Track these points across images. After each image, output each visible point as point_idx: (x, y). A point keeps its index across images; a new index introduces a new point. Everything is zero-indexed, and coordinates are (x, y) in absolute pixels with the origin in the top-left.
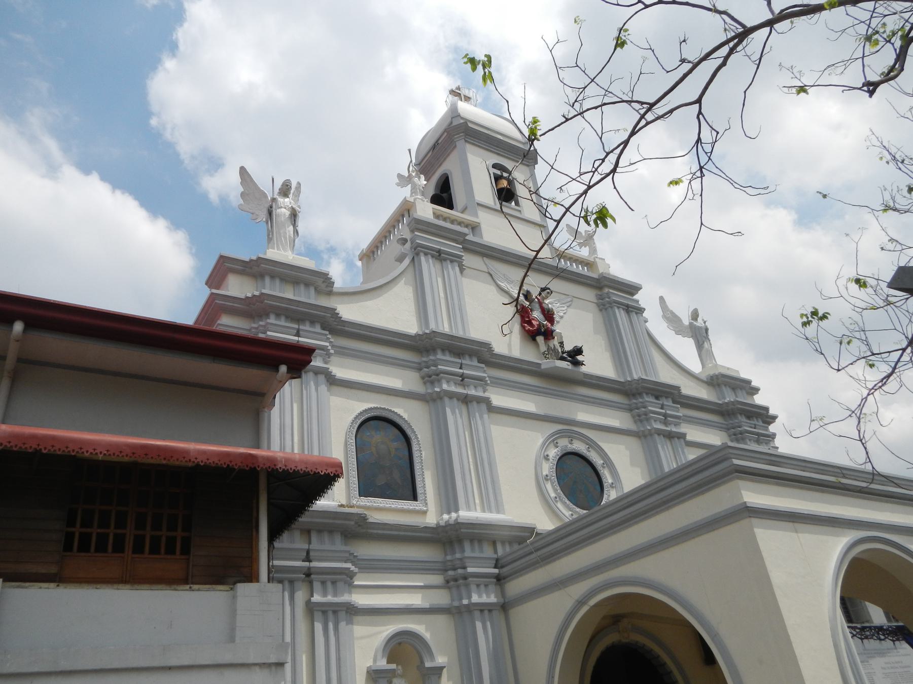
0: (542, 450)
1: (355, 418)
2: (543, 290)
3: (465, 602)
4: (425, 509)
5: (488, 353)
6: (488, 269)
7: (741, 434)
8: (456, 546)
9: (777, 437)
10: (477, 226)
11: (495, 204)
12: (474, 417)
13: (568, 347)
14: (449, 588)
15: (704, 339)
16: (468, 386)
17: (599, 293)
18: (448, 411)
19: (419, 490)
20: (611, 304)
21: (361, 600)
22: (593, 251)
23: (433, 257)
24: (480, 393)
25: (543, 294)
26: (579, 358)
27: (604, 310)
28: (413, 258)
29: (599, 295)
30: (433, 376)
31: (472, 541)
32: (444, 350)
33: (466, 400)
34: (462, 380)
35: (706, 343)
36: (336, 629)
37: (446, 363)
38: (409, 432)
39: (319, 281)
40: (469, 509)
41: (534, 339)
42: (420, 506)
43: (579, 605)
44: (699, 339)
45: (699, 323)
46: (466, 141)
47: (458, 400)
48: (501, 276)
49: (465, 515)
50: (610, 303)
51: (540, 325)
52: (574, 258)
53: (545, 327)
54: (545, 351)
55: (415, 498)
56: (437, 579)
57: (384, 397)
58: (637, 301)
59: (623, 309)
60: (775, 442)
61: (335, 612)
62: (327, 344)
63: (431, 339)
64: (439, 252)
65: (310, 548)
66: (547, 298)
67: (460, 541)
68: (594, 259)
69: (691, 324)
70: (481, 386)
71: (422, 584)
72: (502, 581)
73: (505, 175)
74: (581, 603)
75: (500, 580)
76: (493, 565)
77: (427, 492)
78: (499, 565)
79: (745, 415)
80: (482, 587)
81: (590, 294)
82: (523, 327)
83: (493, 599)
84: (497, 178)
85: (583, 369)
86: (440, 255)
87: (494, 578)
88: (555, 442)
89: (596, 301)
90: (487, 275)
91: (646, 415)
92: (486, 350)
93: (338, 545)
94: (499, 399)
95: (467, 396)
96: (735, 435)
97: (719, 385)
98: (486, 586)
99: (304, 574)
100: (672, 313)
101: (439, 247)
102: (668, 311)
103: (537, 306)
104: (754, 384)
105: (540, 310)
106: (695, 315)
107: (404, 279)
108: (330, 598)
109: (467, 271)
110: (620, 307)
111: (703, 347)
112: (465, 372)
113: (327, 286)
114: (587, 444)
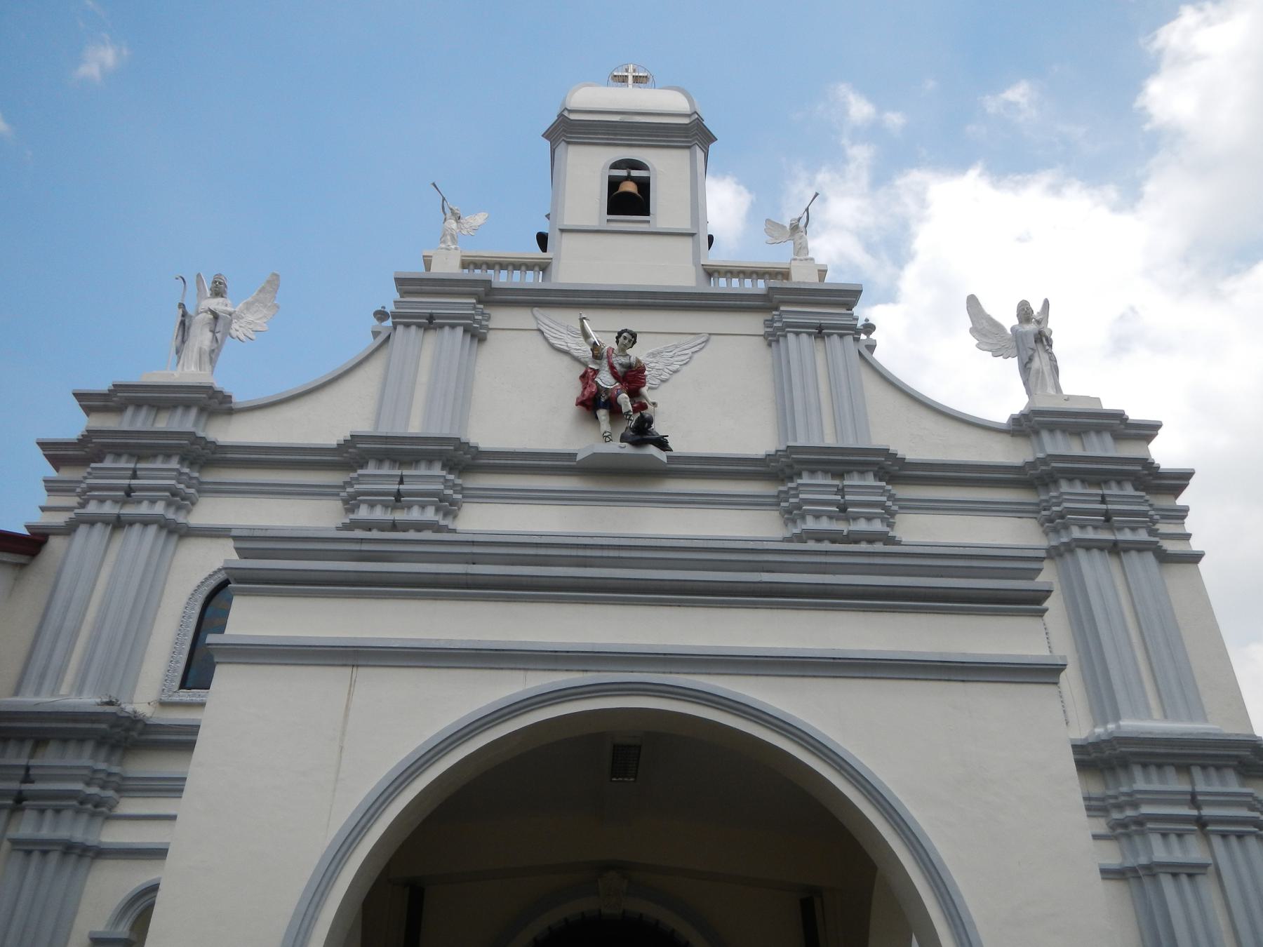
2: (620, 334)
7: (1062, 517)
9: (1189, 513)
23: (419, 326)
25: (621, 339)
27: (774, 344)
28: (389, 336)
29: (767, 320)
46: (569, 143)
48: (562, 330)
53: (610, 395)
54: (605, 432)
59: (809, 334)
60: (1185, 525)
61: (45, 853)
64: (431, 318)
70: (432, 503)
73: (635, 173)
79: (1083, 481)
81: (754, 323)
84: (614, 184)
85: (679, 446)
90: (537, 333)
91: (800, 508)
93: (83, 758)
96: (1051, 521)
97: (1037, 433)
101: (429, 311)
103: (605, 362)
104: (1134, 414)
105: (607, 369)
108: (46, 833)
109: (491, 336)
110: (801, 332)
111: (1030, 368)
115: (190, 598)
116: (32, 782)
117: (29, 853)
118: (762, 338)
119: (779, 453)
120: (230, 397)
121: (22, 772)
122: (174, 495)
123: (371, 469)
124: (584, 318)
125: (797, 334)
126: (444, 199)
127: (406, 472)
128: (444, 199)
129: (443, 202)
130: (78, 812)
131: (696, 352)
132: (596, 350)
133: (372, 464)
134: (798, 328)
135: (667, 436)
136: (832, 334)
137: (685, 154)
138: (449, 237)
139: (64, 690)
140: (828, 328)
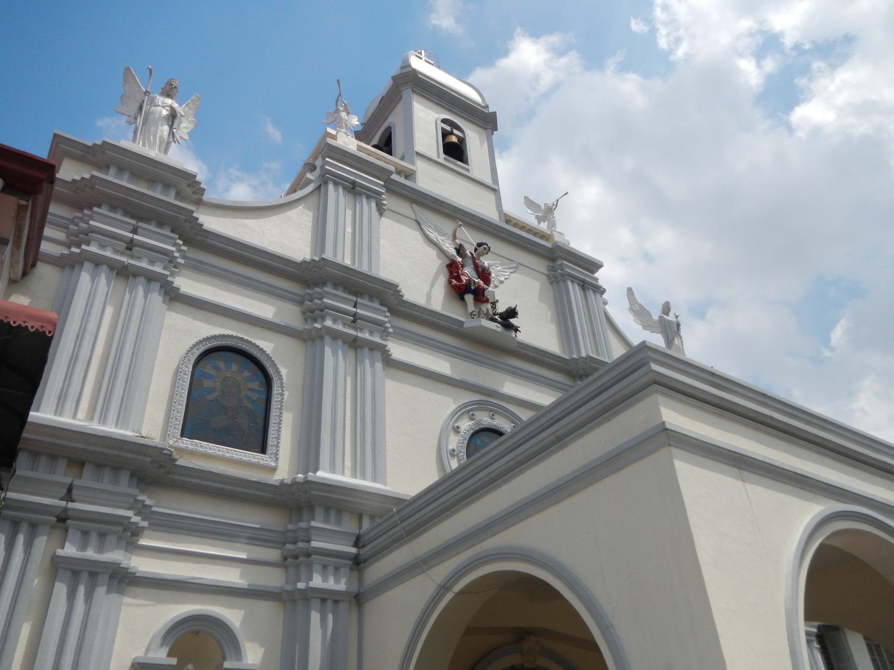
0: (451, 419)
1: (200, 342)
2: (480, 245)
3: (301, 585)
4: (273, 464)
5: (394, 297)
6: (416, 216)
8: (306, 514)
10: (412, 174)
11: (439, 156)
12: (363, 362)
13: (501, 308)
14: (286, 567)
15: (674, 334)
17: (551, 264)
18: (328, 351)
19: (271, 441)
20: (564, 277)
21: (143, 565)
22: (553, 225)
23: (344, 188)
24: (377, 339)
25: (481, 249)
26: (513, 321)
27: (555, 283)
28: (320, 186)
29: (551, 266)
31: (327, 509)
32: (335, 286)
33: (355, 344)
34: (354, 322)
35: (676, 339)
36: (89, 596)
37: (335, 299)
38: (271, 371)
39: (184, 185)
40: (333, 470)
42: (266, 460)
43: (443, 591)
44: (670, 335)
45: (671, 317)
46: (413, 91)
47: (344, 342)
48: (432, 226)
49: (323, 474)
50: (562, 276)
51: (469, 281)
52: (528, 228)
53: (477, 285)
54: (474, 312)
56: (272, 554)
57: (246, 327)
58: (597, 279)
59: (578, 284)
61: (93, 575)
62: (173, 249)
63: (320, 269)
64: (354, 183)
65: (74, 483)
66: (483, 254)
67: (311, 508)
68: (552, 232)
69: (661, 317)
71: (243, 556)
72: (362, 565)
73: (455, 131)
74: (444, 588)
75: (358, 563)
77: (281, 445)
78: (361, 545)
80: (331, 569)
81: (541, 265)
82: (450, 282)
83: (342, 586)
84: (445, 134)
85: (521, 337)
86: (353, 188)
87: (351, 560)
88: (471, 413)
89: (546, 273)
90: (415, 223)
92: (392, 292)
93: (124, 486)
94: (399, 351)
95: (356, 339)
98: (337, 568)
99: (56, 517)
100: (641, 306)
101: (354, 178)
102: (636, 304)
103: (470, 261)
105: (472, 266)
106: (666, 309)
107: (302, 205)
108: (91, 554)
109: (386, 213)
111: (673, 344)
112: (359, 311)
113: (194, 193)
114: (513, 423)
115: (185, 357)
116: (73, 501)
117: (76, 573)
118: (545, 276)
119: (582, 359)
121: (65, 491)
122: (170, 261)
123: (329, 289)
124: (462, 225)
125: (572, 282)
126: (340, 95)
127: (359, 300)
128: (340, 95)
129: (339, 96)
130: (120, 538)
131: (511, 273)
132: (460, 250)
133: (329, 285)
134: (574, 279)
137: (483, 132)
138: (344, 125)
139: (81, 414)
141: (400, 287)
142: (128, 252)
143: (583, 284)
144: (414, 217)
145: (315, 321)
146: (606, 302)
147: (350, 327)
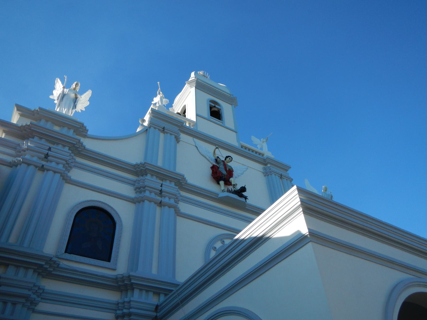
2: (227, 157)
13: (238, 187)
16: (165, 197)
25: (228, 159)
26: (244, 194)
27: (266, 176)
30: (141, 189)
41: (219, 184)
47: (155, 203)
54: (224, 189)
55: (109, 261)
76: (154, 309)
86: (163, 131)
89: (262, 171)
120: (88, 131)
134: (276, 173)
135: (248, 197)
136: (285, 178)
140: (284, 176)
141: (185, 176)
142: (45, 159)
143: (281, 176)
144: (195, 145)
145: (140, 192)
146: (293, 185)
147: (158, 196)
